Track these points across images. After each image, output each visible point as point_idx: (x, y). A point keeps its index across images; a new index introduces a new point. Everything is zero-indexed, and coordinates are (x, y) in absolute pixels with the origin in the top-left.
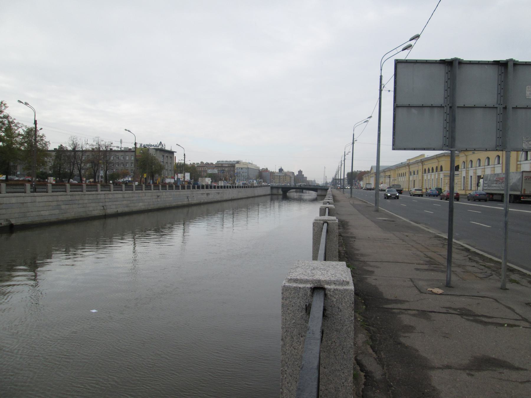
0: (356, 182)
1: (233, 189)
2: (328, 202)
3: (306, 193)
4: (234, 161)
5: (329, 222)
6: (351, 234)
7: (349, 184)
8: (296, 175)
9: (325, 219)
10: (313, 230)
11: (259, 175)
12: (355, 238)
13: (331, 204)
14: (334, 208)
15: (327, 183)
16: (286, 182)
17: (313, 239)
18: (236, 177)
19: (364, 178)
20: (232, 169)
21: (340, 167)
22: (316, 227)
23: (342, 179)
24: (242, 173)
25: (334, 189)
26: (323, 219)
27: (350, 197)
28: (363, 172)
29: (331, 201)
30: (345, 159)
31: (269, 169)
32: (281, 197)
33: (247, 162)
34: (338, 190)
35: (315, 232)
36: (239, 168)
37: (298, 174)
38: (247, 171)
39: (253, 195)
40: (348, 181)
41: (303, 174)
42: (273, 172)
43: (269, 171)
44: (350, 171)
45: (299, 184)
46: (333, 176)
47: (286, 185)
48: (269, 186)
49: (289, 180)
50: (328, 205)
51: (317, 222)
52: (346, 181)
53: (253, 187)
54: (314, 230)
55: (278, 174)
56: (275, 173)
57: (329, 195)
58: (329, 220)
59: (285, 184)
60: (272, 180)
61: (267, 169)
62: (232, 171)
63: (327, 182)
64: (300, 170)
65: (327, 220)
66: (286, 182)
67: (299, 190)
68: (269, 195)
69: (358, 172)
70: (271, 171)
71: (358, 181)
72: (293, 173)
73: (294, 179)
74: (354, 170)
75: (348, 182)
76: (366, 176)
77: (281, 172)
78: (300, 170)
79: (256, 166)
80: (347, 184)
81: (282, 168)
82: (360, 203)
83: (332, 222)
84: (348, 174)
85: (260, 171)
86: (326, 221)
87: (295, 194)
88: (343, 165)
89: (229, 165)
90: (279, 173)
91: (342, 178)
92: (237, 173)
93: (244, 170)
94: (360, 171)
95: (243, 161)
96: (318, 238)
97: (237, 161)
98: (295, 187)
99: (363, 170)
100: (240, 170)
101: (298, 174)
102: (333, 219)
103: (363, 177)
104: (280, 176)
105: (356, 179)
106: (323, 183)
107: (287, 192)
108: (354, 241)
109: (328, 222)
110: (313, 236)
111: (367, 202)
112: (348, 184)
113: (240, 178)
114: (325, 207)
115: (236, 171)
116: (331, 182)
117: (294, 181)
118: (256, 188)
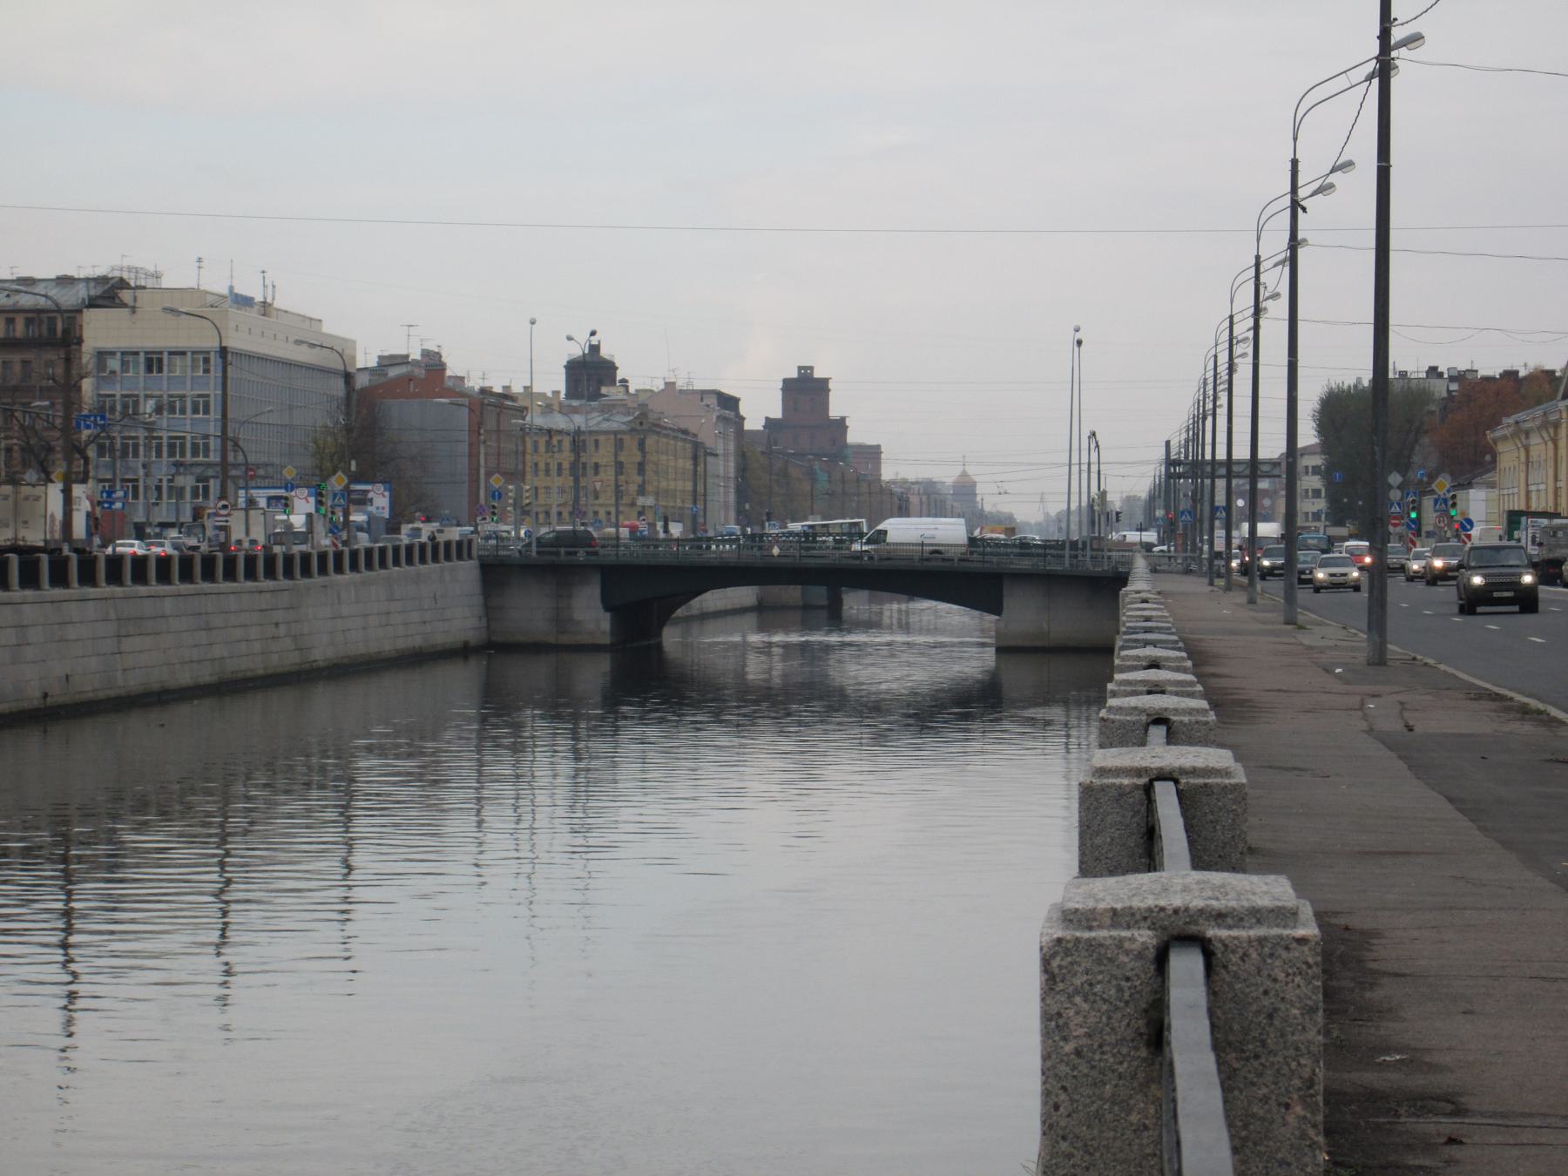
0: (1424, 490)
1: (58, 592)
2: (1160, 720)
3: (871, 625)
4: (65, 281)
5: (1224, 933)
6: (1415, 1061)
7: (1339, 523)
8: (754, 422)
9: (1178, 902)
10: (1046, 1034)
11: (348, 429)
12: (1460, 1111)
13: (1191, 741)
14: (1240, 778)
15: (1099, 513)
16: (648, 501)
17: (1049, 1127)
18: (92, 452)
19: (1509, 455)
20: (47, 363)
21: (1243, 327)
22: (1077, 992)
23: (1274, 464)
24: (159, 410)
25: (1188, 572)
26: (1150, 902)
27: (1361, 657)
28: (1488, 380)
29: (1190, 712)
30: (1294, 243)
31: (454, 368)
32: (593, 674)
33: (216, 283)
34: (1228, 588)
35: (1069, 1048)
36: (128, 355)
37: (777, 413)
38: (214, 392)
39: (284, 657)
40: (1329, 484)
41: (835, 411)
42: (506, 395)
43: (456, 390)
44: (1356, 370)
45: (796, 527)
46: (1171, 426)
47: (652, 541)
48: (461, 550)
49: (689, 486)
50: (1158, 754)
51: (1086, 935)
52: (1315, 482)
53: (1546, 490)
54: (1053, 1024)
55: (559, 422)
56: (522, 411)
57: (1146, 643)
58: (1220, 917)
59: (643, 527)
60: (497, 481)
61: (433, 364)
62: (44, 392)
63: (1103, 495)
64: (805, 376)
65: (1201, 911)
66: (648, 501)
67: (792, 593)
68: (463, 652)
69: (1440, 389)
70: (474, 383)
71: (1443, 484)
72: (729, 403)
73: (743, 469)
74: (1406, 359)
75: (1333, 499)
76: (1521, 433)
77: (597, 395)
78: (805, 376)
79: (307, 330)
80: (1317, 516)
81: (605, 352)
82: (1477, 722)
83: (1261, 931)
84: (1335, 407)
85: (362, 381)
86: (1193, 929)
87: (755, 638)
88: (1277, 311)
89: (10, 321)
90: (566, 410)
91: (1273, 446)
92: (102, 410)
93: (182, 381)
94: (1459, 377)
95: (166, 283)
96: (1098, 1116)
97: (103, 280)
98: (753, 556)
99: (1490, 366)
100: (137, 380)
101: (777, 413)
102: (1264, 902)
103: (1490, 435)
104: (578, 441)
105: (1425, 455)
106: (1056, 507)
107: (665, 617)
108: (1452, 1141)
109: (1212, 932)
110: (1046, 1094)
111: (1554, 712)
112: (1338, 515)
113: (137, 464)
114: (1138, 772)
115: (87, 385)
116: (1152, 498)
117: (742, 493)
118: (318, 580)
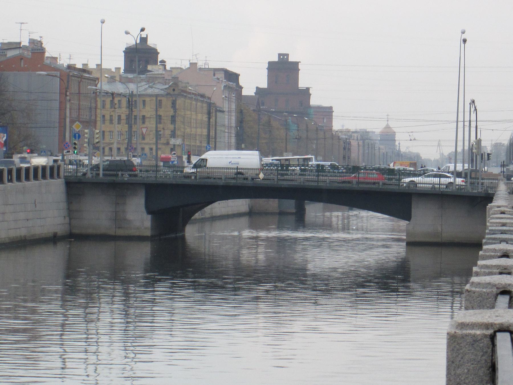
3: (328, 226)
16: (178, 141)
37: (264, 84)
41: (302, 84)
42: (84, 70)
49: (205, 132)
55: (120, 88)
56: (95, 80)
57: (501, 241)
59: (173, 158)
60: (77, 127)
63: (479, 142)
64: (283, 58)
66: (178, 141)
70: (64, 62)
73: (241, 121)
77: (144, 71)
78: (283, 58)
81: (151, 42)
87: (247, 233)
90: (124, 81)
101: (264, 84)
107: (187, 219)
114: (487, 326)
